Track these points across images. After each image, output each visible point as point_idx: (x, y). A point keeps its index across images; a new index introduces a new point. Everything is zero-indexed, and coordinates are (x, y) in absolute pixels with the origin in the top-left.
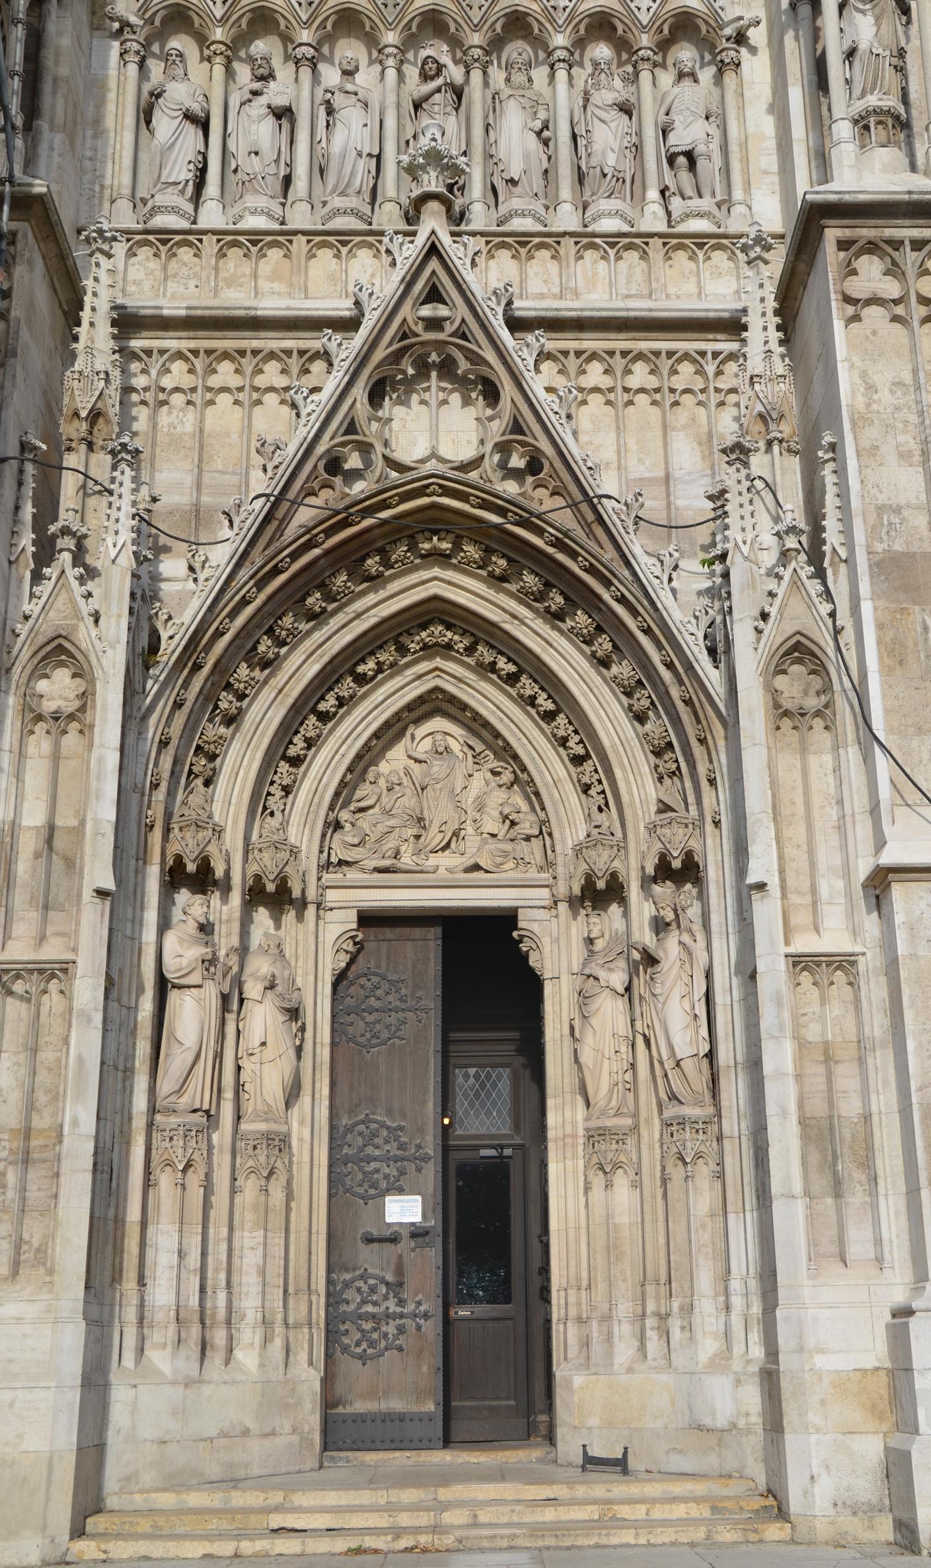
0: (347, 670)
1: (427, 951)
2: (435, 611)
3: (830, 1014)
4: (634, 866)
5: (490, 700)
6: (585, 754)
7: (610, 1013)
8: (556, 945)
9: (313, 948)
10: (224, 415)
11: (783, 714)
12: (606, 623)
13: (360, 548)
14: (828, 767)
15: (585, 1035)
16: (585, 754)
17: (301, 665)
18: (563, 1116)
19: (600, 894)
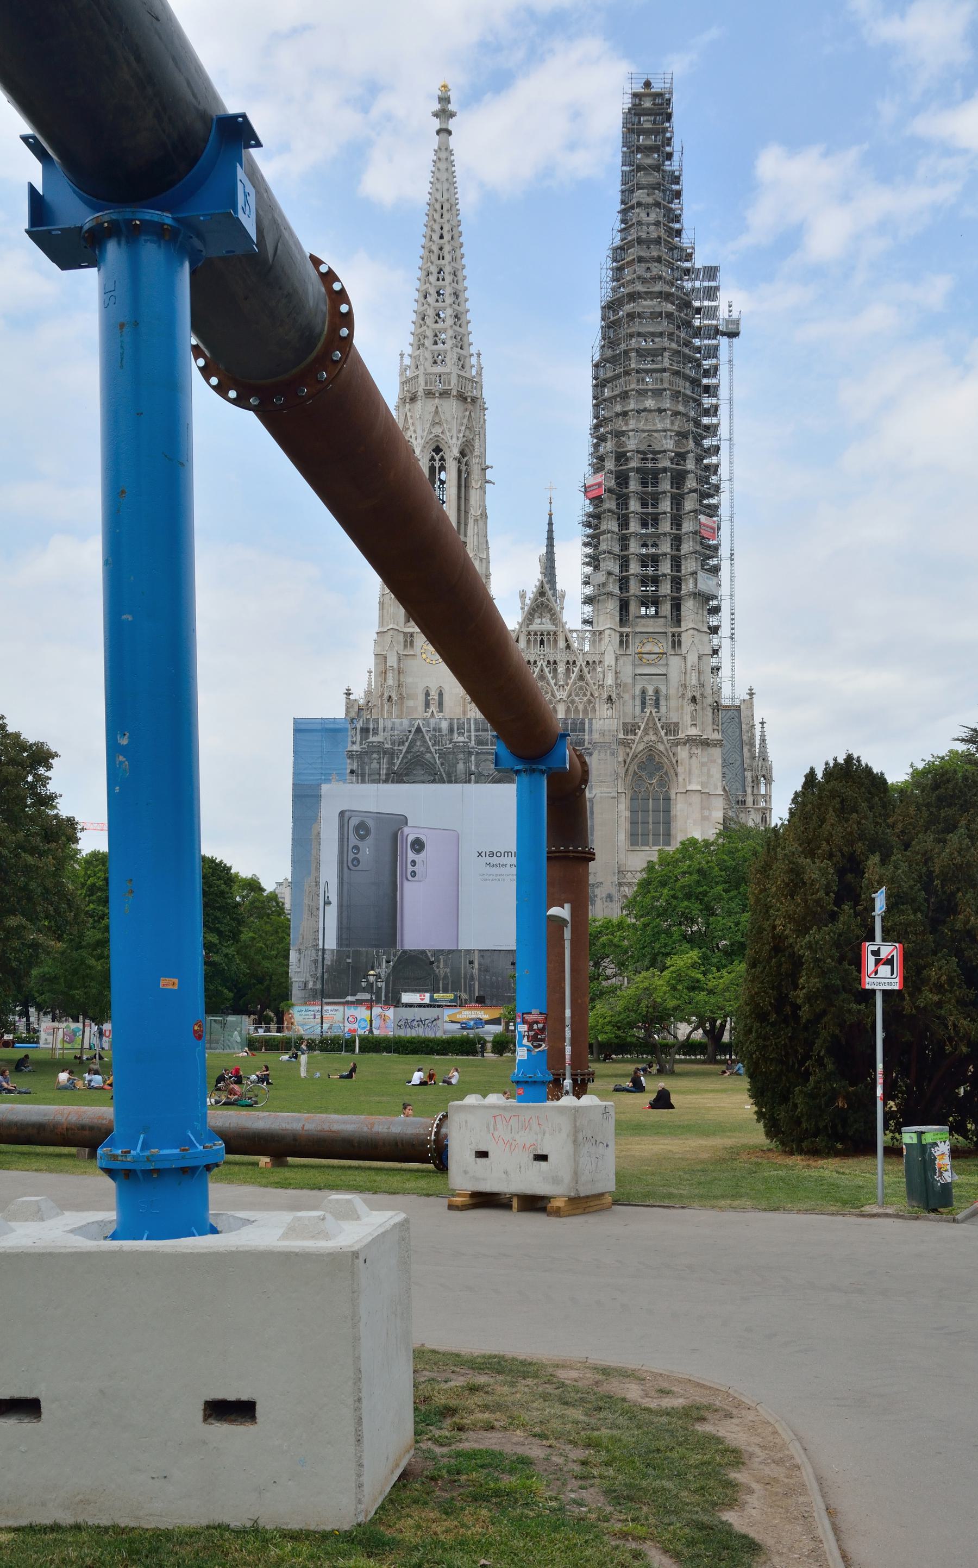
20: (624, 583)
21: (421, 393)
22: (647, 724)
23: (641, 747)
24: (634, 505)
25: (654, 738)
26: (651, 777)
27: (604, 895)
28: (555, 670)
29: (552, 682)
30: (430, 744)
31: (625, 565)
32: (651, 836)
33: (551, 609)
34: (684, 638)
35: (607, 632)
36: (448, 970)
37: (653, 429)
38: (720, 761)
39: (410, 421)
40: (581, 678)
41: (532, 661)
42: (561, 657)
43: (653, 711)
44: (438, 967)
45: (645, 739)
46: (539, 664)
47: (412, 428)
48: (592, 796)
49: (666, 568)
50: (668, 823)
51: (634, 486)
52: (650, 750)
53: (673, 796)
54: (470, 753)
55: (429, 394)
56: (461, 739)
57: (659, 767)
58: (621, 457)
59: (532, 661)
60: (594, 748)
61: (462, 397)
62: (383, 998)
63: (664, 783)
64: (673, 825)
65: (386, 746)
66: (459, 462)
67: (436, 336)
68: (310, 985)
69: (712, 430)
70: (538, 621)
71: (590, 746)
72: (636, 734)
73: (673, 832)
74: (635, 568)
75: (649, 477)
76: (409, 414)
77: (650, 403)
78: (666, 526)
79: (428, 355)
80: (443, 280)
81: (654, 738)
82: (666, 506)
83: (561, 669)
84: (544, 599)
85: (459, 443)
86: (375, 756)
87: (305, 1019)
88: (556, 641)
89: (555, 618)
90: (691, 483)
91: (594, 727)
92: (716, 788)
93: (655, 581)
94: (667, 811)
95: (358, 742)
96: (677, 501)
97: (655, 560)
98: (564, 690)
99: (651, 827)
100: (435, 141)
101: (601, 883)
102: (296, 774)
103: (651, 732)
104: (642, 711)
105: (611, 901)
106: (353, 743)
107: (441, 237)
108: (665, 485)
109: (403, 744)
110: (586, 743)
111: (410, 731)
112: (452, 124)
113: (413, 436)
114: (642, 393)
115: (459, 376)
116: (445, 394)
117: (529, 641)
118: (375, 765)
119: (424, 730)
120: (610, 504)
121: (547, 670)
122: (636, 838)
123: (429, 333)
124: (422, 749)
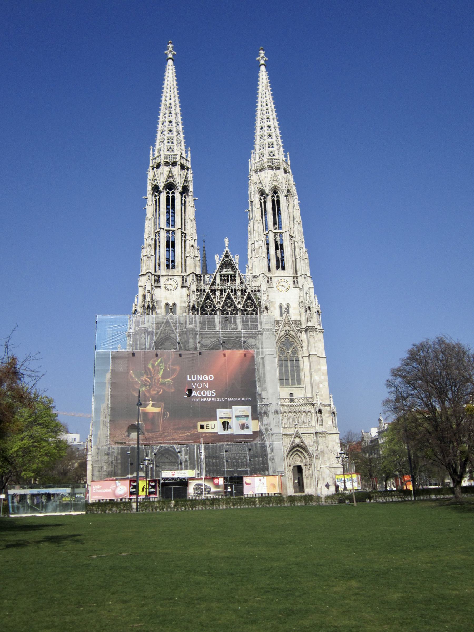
0: (293, 453)
1: (296, 468)
2: (297, 450)
3: (318, 473)
4: (308, 464)
5: (299, 454)
6: (305, 457)
7: (307, 472)
8: (303, 467)
9: (292, 467)
10: (286, 439)
11: (316, 459)
12: (306, 451)
13: (294, 447)
14: (318, 461)
15: (305, 473)
16: (305, 457)
17: (291, 453)
18: (304, 477)
19: (306, 465)
21: (162, 162)
22: (284, 321)
23: (283, 333)
25: (288, 328)
26: (288, 349)
27: (273, 410)
28: (235, 294)
29: (234, 300)
30: (174, 329)
32: (290, 380)
33: (232, 264)
34: (299, 279)
35: (262, 276)
36: (187, 457)
38: (323, 340)
39: (156, 175)
40: (249, 298)
41: (223, 288)
43: (288, 315)
44: (181, 455)
45: (285, 329)
46: (227, 291)
47: (157, 179)
48: (263, 356)
50: (298, 373)
52: (287, 335)
53: (300, 359)
54: (196, 334)
55: (167, 164)
56: (191, 326)
57: (292, 343)
59: (223, 288)
60: (263, 331)
62: (150, 475)
63: (295, 351)
64: (302, 374)
65: (149, 330)
66: (182, 196)
67: (168, 139)
68: (105, 468)
70: (226, 270)
71: (261, 330)
72: (279, 326)
73: (302, 377)
76: (156, 172)
79: (165, 147)
80: (172, 116)
81: (288, 328)
83: (239, 293)
84: (228, 259)
85: (182, 185)
86: (143, 335)
88: (235, 280)
89: (233, 269)
91: (262, 320)
92: (322, 354)
94: (298, 367)
95: (133, 328)
98: (241, 304)
99: (290, 375)
101: (271, 404)
103: (287, 325)
104: (281, 315)
105: (277, 414)
106: (131, 328)
107: (170, 99)
109: (159, 329)
110: (259, 328)
111: (163, 322)
113: (158, 182)
115: (181, 156)
116: (174, 164)
117: (221, 280)
118: (143, 339)
119: (170, 321)
121: (231, 294)
122: (284, 381)
123: (166, 138)
124: (170, 332)
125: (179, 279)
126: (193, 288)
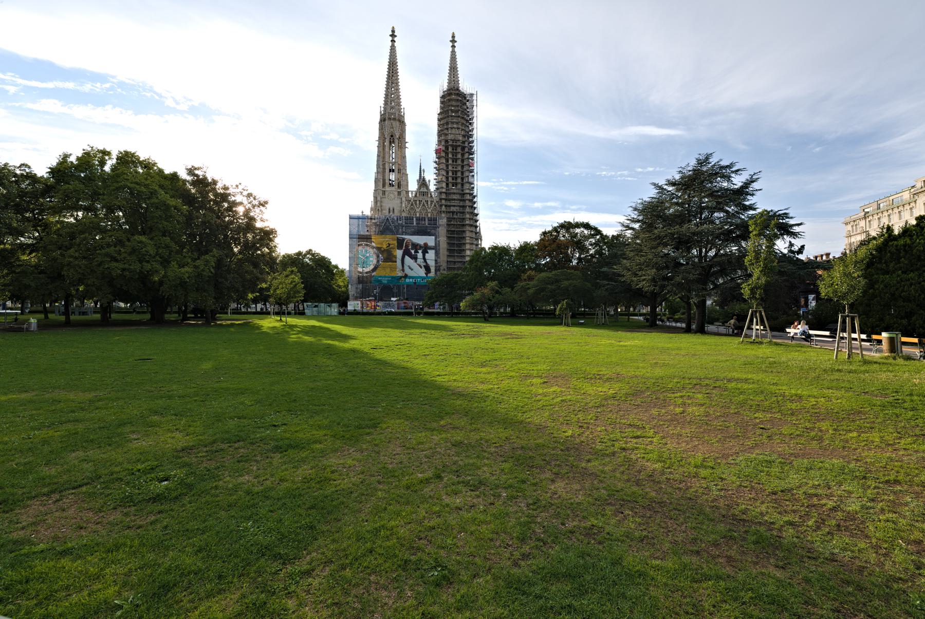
20: (447, 178)
24: (450, 156)
31: (447, 173)
37: (455, 134)
42: (429, 200)
49: (459, 174)
51: (450, 149)
55: (390, 119)
58: (447, 141)
61: (400, 121)
69: (471, 136)
74: (450, 174)
75: (455, 147)
77: (455, 126)
78: (459, 162)
82: (459, 156)
87: (352, 305)
90: (466, 150)
93: (456, 178)
96: (463, 155)
97: (456, 172)
100: (390, 44)
102: (350, 231)
108: (459, 150)
112: (395, 39)
114: (453, 123)
116: (394, 119)
120: (443, 154)
125: (396, 193)
126: (404, 199)
